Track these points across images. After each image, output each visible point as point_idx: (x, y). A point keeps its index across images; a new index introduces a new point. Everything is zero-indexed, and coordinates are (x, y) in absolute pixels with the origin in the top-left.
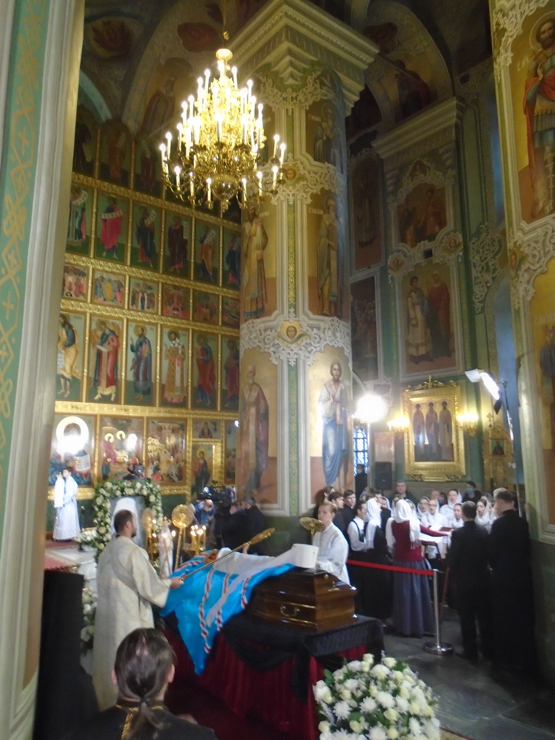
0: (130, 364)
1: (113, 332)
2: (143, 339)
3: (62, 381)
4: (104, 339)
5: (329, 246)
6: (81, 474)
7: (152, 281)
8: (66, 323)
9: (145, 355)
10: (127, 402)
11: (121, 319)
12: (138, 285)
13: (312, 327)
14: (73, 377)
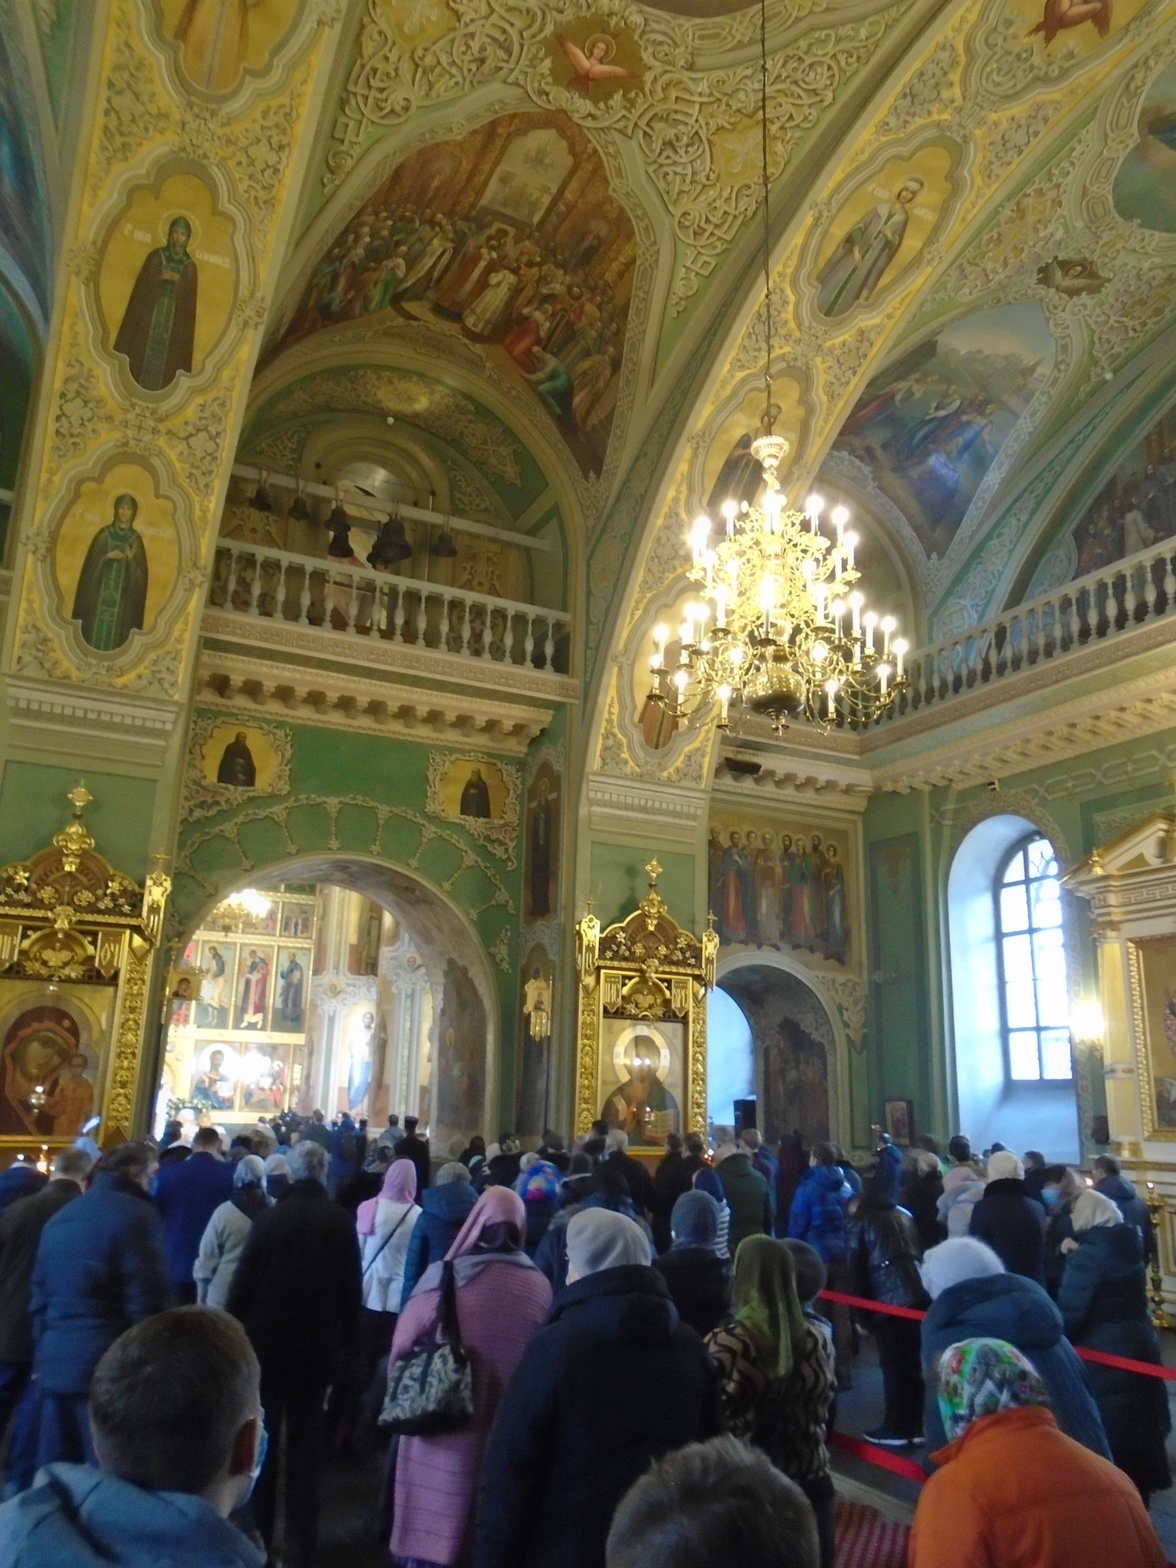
0: (279, 991)
1: (263, 960)
2: (294, 966)
3: (210, 1009)
4: (253, 967)
5: (371, 917)
6: (224, 1099)
7: (307, 905)
8: (216, 955)
9: (295, 981)
10: (274, 1029)
11: (272, 947)
12: (292, 911)
13: (348, 985)
14: (221, 1006)
